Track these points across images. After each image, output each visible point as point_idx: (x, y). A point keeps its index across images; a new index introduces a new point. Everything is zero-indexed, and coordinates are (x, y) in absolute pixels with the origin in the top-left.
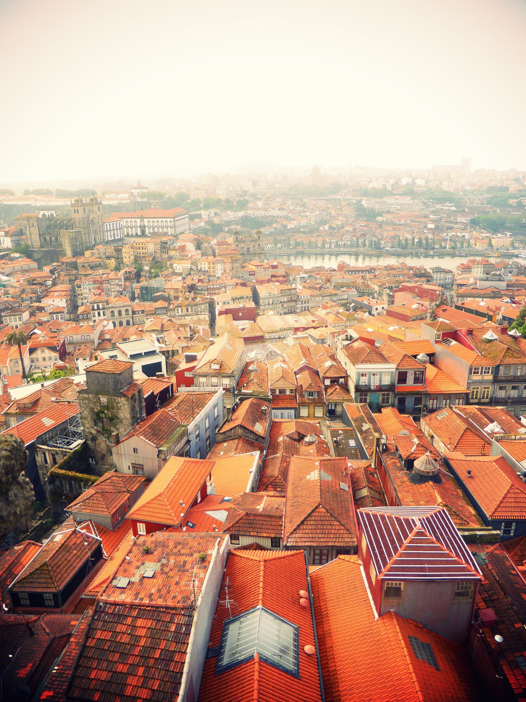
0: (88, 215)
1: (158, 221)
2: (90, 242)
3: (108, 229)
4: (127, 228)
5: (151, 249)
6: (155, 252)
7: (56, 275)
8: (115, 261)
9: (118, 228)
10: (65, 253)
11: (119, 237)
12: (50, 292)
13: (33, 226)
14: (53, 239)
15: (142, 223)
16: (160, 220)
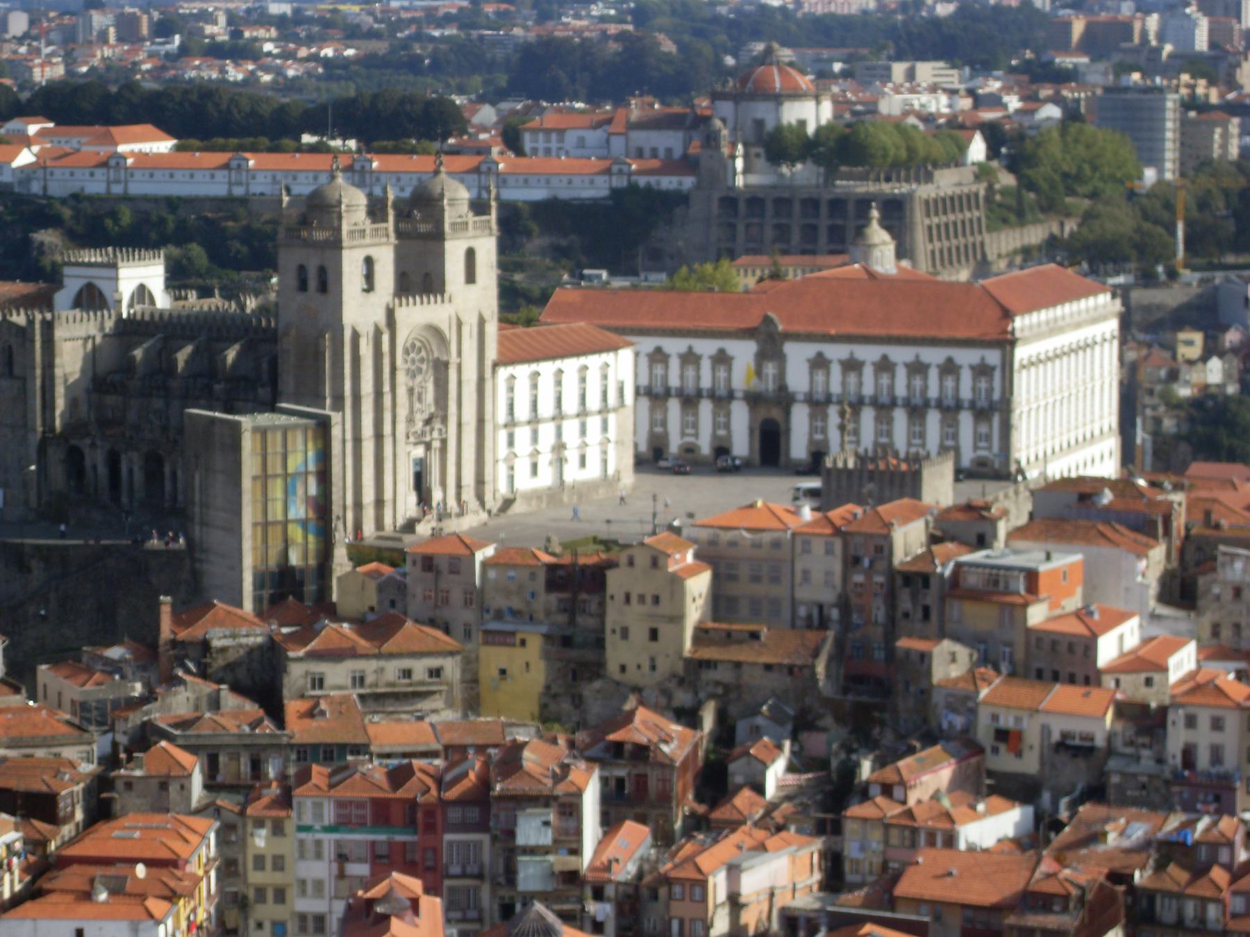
0: (390, 314)
1: (885, 366)
2: (379, 503)
3: (522, 412)
4: (654, 395)
5: (817, 576)
6: (844, 604)
7: (123, 740)
8: (546, 656)
9: (594, 403)
10: (196, 576)
11: (593, 472)
12: (64, 862)
13: (11, 374)
14: (132, 463)
15: (770, 369)
16: (901, 355)
